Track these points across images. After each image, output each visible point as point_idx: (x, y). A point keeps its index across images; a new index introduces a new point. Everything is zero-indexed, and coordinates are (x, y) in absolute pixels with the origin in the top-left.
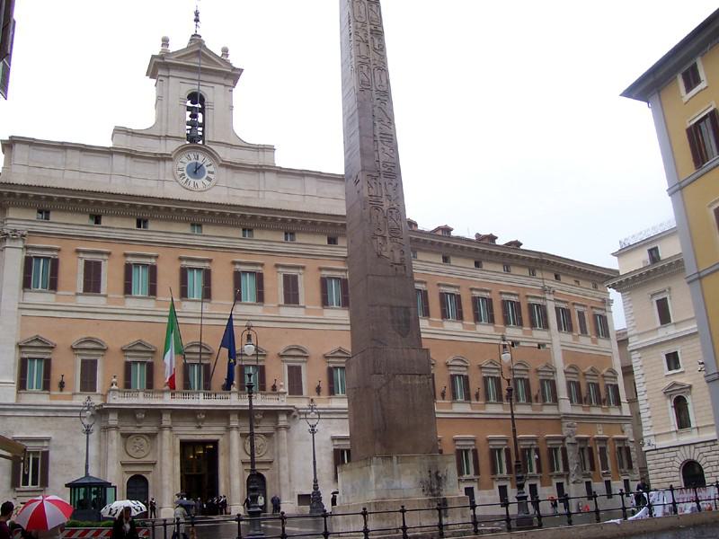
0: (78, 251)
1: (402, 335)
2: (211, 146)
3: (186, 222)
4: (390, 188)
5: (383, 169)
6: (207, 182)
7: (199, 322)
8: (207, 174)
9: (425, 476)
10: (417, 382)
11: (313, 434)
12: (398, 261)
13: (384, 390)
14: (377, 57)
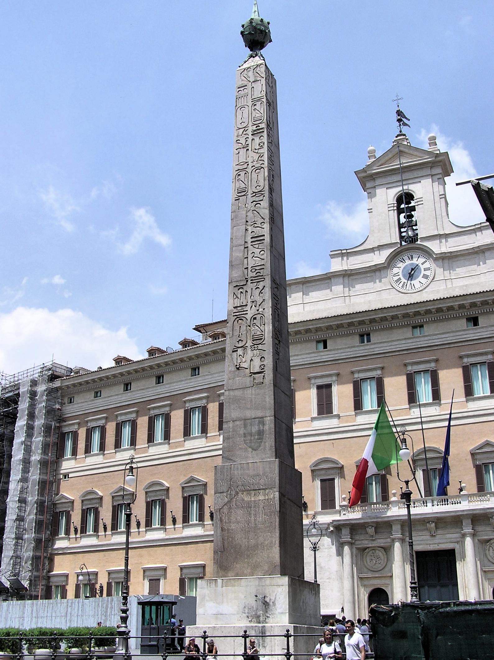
0: (309, 379)
1: (253, 449)
2: (425, 244)
3: (407, 326)
4: (258, 291)
5: (251, 274)
6: (424, 281)
7: (419, 427)
8: (423, 272)
9: (252, 602)
10: (261, 497)
11: (315, 551)
12: (257, 369)
13: (225, 510)
14: (256, 156)
